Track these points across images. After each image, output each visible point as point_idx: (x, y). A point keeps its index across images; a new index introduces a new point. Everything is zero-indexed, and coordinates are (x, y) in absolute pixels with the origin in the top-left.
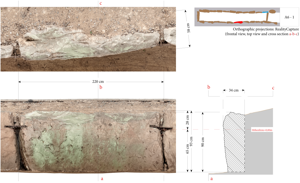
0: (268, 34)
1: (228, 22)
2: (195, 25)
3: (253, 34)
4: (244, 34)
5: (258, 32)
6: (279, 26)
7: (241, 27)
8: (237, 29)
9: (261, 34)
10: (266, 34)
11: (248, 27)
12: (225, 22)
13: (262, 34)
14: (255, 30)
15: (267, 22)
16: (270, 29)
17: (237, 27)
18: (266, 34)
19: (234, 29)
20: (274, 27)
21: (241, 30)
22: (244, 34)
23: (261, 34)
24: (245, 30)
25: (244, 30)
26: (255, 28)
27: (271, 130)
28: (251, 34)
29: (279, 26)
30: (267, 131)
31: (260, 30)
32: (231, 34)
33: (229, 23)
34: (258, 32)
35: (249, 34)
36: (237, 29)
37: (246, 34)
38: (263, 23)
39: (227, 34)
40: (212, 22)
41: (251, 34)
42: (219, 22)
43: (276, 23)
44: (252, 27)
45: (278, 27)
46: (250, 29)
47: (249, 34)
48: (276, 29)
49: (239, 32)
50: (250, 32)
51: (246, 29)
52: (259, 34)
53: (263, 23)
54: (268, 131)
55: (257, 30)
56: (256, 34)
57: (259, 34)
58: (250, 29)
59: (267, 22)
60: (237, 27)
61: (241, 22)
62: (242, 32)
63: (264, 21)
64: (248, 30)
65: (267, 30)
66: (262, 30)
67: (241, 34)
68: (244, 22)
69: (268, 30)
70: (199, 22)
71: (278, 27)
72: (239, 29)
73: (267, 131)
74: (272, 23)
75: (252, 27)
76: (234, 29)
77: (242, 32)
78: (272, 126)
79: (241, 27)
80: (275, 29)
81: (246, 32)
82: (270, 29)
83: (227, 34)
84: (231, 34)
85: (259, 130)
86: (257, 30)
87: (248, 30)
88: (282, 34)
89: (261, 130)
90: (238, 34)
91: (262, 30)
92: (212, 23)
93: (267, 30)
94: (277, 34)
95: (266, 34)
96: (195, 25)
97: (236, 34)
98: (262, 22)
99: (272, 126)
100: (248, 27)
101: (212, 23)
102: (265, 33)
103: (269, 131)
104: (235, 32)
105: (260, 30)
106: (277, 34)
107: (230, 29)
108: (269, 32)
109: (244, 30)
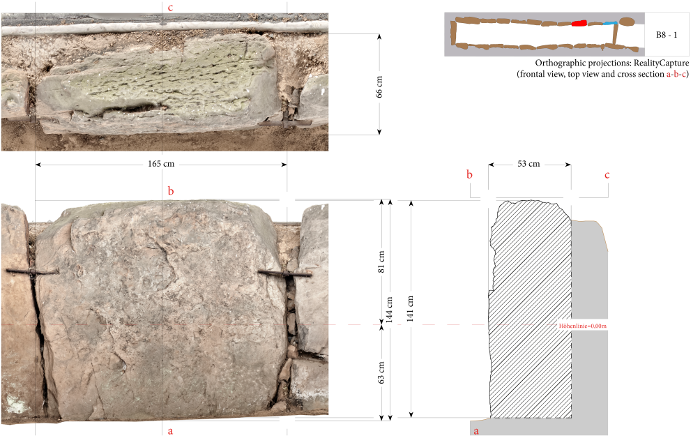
0: (616, 75)
1: (524, 47)
2: (447, 54)
3: (581, 75)
4: (561, 75)
5: (594, 69)
6: (643, 55)
7: (554, 59)
9: (600, 75)
10: (612, 75)
11: (572, 59)
13: (603, 75)
14: (587, 64)
15: (614, 47)
16: (622, 64)
17: (544, 59)
18: (613, 75)
19: (539, 63)
20: (631, 59)
21: (553, 64)
22: (561, 75)
23: (600, 75)
24: (562, 64)
25: (560, 65)
26: (586, 59)
27: (605, 326)
28: (576, 75)
29: (643, 55)
30: (593, 329)
31: (598, 64)
32: (532, 75)
33: (526, 49)
34: (594, 69)
35: (573, 75)
37: (566, 74)
38: (606, 47)
39: (522, 74)
40: (486, 47)
41: (576, 75)
42: (501, 46)
43: (635, 49)
44: (578, 59)
45: (641, 59)
46: (576, 63)
47: (573, 75)
48: (636, 63)
49: (548, 69)
50: (575, 69)
51: (565, 64)
52: (596, 75)
53: (606, 47)
54: (596, 329)
56: (589, 75)
57: (596, 75)
58: (576, 63)
59: (614, 47)
60: (544, 59)
61: (553, 47)
62: (556, 69)
63: (608, 45)
64: (570, 64)
65: (614, 64)
66: (603, 64)
67: (554, 75)
68: (560, 46)
69: (616, 64)
70: (455, 47)
71: (641, 59)
72: (549, 63)
73: (593, 329)
74: (626, 48)
75: (578, 59)
76: (539, 63)
77: (556, 69)
78: (605, 316)
79: (554, 59)
80: (633, 63)
81: (565, 69)
82: (622, 64)
83: (522, 74)
84: (532, 75)
85: (577, 326)
87: (570, 64)
89: (581, 326)
90: (546, 75)
91: (603, 64)
92: (485, 49)
93: (614, 64)
94: (637, 75)
95: (613, 75)
96: (447, 54)
97: (542, 75)
98: (602, 46)
99: (605, 316)
100: (572, 59)
101: (485, 49)
103: (598, 329)
104: (540, 69)
105: (598, 64)
106: (637, 75)
108: (619, 69)
109: (560, 65)
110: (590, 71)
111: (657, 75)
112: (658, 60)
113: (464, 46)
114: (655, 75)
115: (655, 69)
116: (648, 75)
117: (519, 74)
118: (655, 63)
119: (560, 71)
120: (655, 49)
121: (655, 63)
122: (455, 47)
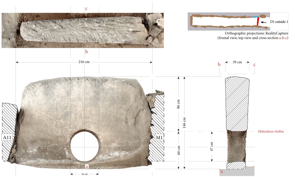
1: (220, 27)
2: (189, 30)
3: (244, 38)
4: (236, 38)
5: (249, 36)
7: (233, 32)
8: (229, 34)
9: (252, 38)
10: (257, 38)
11: (240, 32)
12: (217, 27)
13: (253, 38)
16: (261, 34)
17: (229, 32)
20: (264, 32)
21: (232, 34)
22: (236, 38)
23: (252, 38)
25: (235, 34)
26: (246, 32)
28: (242, 38)
32: (223, 38)
33: (222, 27)
34: (249, 36)
35: (240, 38)
36: (229, 34)
37: (238, 38)
39: (220, 38)
40: (205, 27)
41: (242, 38)
42: (211, 26)
44: (243, 31)
45: (268, 32)
46: (242, 33)
47: (240, 38)
48: (267, 33)
50: (241, 36)
51: (237, 34)
52: (250, 38)
55: (248, 34)
56: (247, 38)
57: (250, 38)
58: (242, 33)
60: (229, 32)
61: (232, 27)
62: (233, 36)
63: (255, 26)
64: (239, 34)
65: (257, 34)
66: (253, 34)
67: (233, 38)
68: (235, 26)
69: (258, 34)
70: (192, 27)
71: (268, 32)
72: (231, 33)
74: (262, 27)
75: (243, 31)
76: (226, 33)
77: (233, 36)
79: (233, 32)
80: (265, 33)
81: (237, 36)
82: (261, 34)
83: (220, 38)
84: (223, 38)
86: (248, 34)
87: (239, 34)
88: (272, 38)
90: (229, 38)
91: (253, 34)
92: (204, 27)
93: (257, 34)
94: (267, 38)
96: (189, 29)
97: (228, 38)
98: (253, 27)
100: (240, 32)
101: (204, 27)
102: (256, 37)
104: (227, 36)
106: (267, 38)
107: (222, 33)
108: (259, 36)
109: (235, 34)
110: (248, 37)
111: (275, 38)
112: (276, 32)
113: (196, 26)
114: (274, 38)
115: (274, 36)
116: (272, 38)
117: (219, 38)
118: (274, 33)
119: (235, 36)
120: (274, 28)
121: (274, 33)
122: (192, 27)
